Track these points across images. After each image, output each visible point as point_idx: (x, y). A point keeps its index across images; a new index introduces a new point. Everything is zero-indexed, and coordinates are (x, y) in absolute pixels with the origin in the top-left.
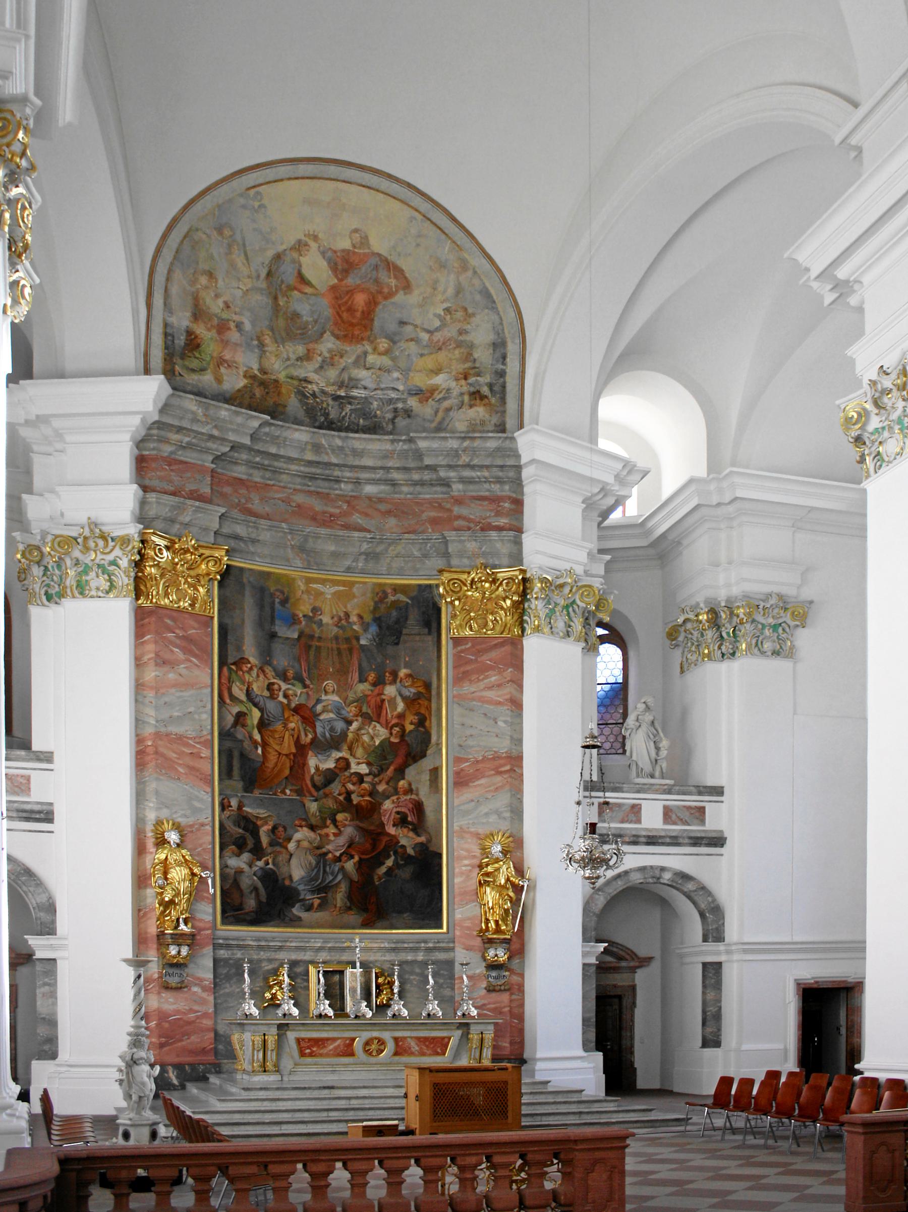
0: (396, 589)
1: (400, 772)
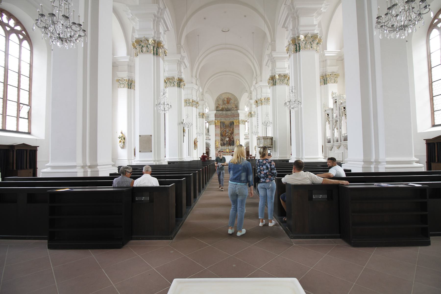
0: (231, 121)
1: (232, 135)
